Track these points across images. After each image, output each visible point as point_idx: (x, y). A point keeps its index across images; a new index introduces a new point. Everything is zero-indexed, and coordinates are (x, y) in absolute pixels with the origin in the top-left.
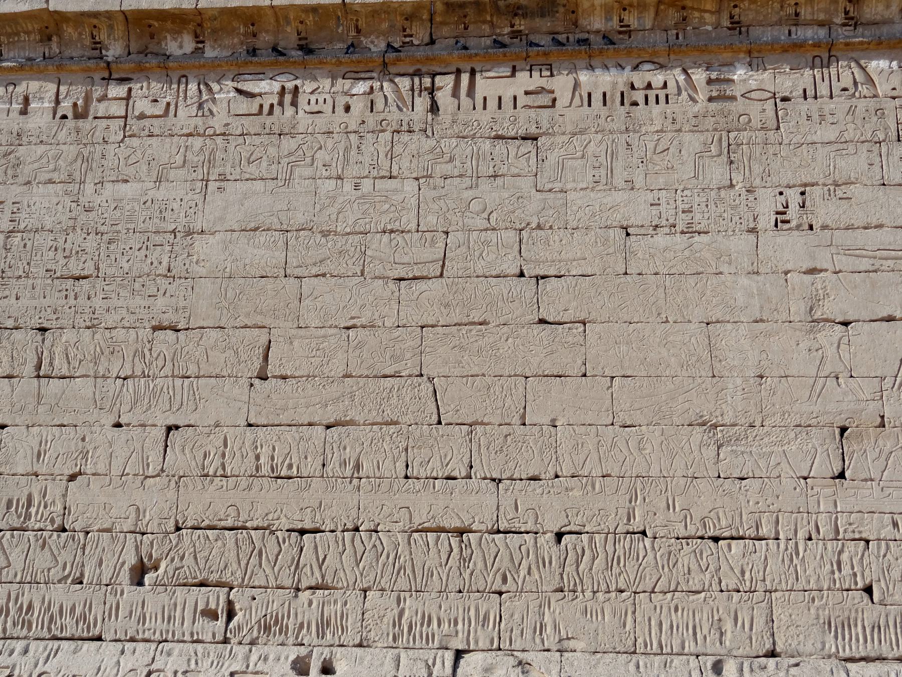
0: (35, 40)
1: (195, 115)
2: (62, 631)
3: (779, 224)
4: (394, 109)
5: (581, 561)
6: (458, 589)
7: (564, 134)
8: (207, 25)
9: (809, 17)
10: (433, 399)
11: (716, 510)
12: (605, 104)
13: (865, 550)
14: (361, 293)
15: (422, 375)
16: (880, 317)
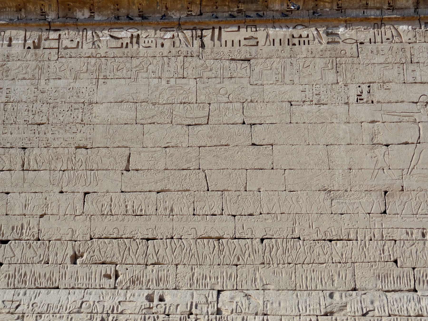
0: (13, 10)
1: (91, 47)
2: (40, 285)
4: (184, 46)
6: (218, 264)
7: (262, 58)
8: (96, 5)
9: (372, 5)
10: (205, 180)
11: (331, 228)
12: (281, 45)
13: (394, 244)
14: (171, 132)
15: (200, 169)
16: (402, 142)
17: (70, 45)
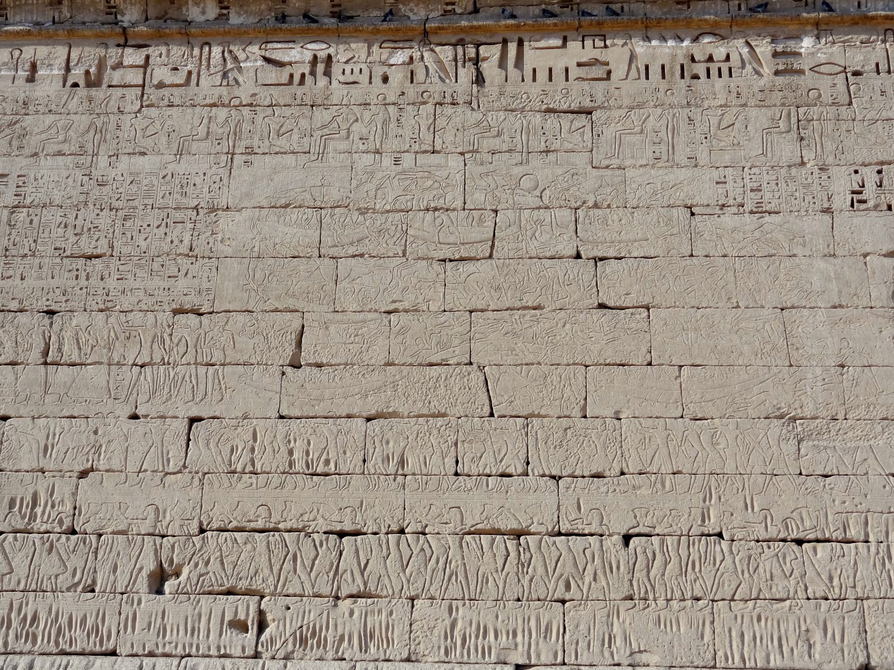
1: (219, 84)
2: (71, 645)
3: (856, 204)
4: (436, 79)
5: (652, 566)
6: (516, 597)
7: (620, 107)
10: (484, 390)
11: (798, 511)
12: (664, 77)
14: (403, 275)
15: (471, 363)
17: (169, 78)
